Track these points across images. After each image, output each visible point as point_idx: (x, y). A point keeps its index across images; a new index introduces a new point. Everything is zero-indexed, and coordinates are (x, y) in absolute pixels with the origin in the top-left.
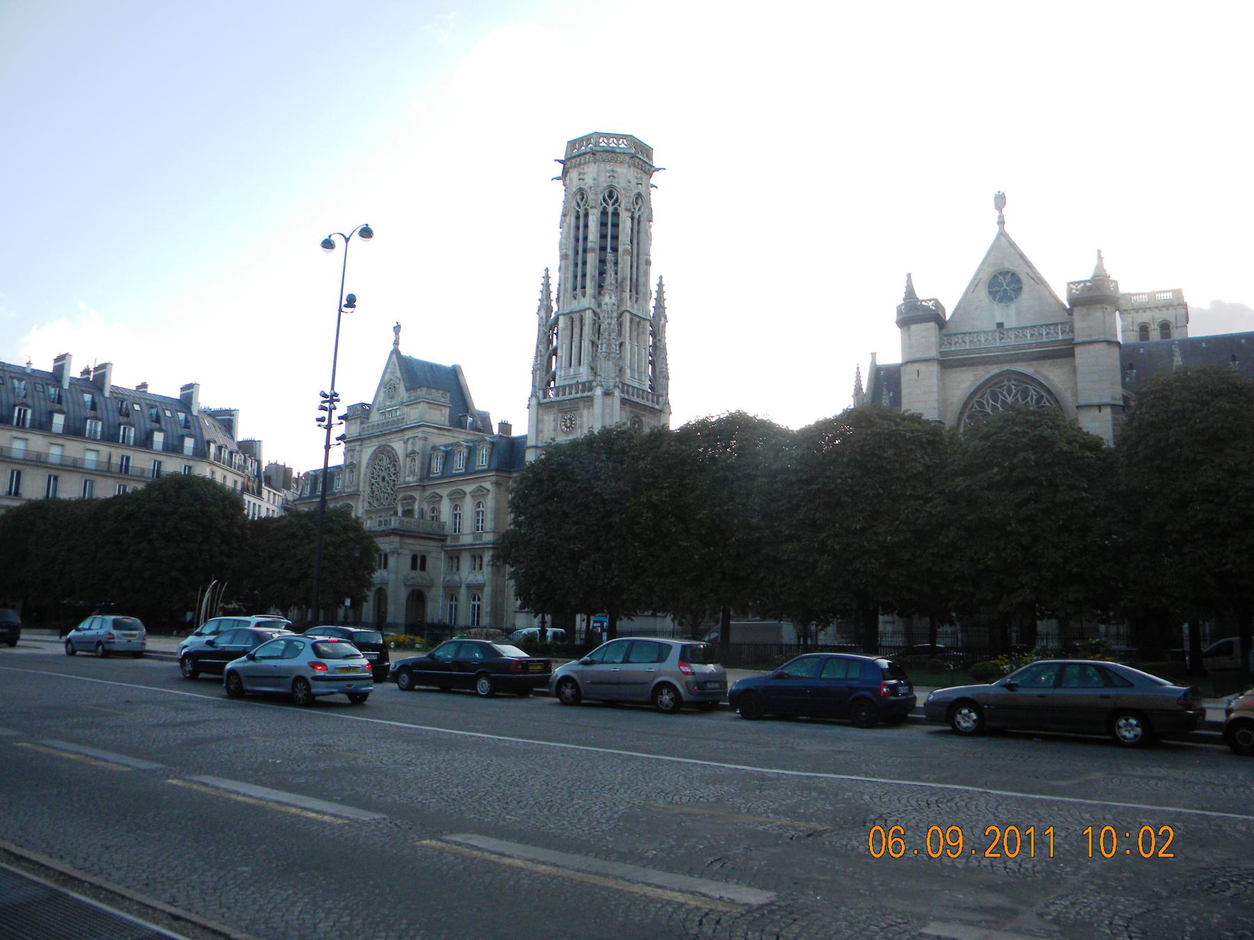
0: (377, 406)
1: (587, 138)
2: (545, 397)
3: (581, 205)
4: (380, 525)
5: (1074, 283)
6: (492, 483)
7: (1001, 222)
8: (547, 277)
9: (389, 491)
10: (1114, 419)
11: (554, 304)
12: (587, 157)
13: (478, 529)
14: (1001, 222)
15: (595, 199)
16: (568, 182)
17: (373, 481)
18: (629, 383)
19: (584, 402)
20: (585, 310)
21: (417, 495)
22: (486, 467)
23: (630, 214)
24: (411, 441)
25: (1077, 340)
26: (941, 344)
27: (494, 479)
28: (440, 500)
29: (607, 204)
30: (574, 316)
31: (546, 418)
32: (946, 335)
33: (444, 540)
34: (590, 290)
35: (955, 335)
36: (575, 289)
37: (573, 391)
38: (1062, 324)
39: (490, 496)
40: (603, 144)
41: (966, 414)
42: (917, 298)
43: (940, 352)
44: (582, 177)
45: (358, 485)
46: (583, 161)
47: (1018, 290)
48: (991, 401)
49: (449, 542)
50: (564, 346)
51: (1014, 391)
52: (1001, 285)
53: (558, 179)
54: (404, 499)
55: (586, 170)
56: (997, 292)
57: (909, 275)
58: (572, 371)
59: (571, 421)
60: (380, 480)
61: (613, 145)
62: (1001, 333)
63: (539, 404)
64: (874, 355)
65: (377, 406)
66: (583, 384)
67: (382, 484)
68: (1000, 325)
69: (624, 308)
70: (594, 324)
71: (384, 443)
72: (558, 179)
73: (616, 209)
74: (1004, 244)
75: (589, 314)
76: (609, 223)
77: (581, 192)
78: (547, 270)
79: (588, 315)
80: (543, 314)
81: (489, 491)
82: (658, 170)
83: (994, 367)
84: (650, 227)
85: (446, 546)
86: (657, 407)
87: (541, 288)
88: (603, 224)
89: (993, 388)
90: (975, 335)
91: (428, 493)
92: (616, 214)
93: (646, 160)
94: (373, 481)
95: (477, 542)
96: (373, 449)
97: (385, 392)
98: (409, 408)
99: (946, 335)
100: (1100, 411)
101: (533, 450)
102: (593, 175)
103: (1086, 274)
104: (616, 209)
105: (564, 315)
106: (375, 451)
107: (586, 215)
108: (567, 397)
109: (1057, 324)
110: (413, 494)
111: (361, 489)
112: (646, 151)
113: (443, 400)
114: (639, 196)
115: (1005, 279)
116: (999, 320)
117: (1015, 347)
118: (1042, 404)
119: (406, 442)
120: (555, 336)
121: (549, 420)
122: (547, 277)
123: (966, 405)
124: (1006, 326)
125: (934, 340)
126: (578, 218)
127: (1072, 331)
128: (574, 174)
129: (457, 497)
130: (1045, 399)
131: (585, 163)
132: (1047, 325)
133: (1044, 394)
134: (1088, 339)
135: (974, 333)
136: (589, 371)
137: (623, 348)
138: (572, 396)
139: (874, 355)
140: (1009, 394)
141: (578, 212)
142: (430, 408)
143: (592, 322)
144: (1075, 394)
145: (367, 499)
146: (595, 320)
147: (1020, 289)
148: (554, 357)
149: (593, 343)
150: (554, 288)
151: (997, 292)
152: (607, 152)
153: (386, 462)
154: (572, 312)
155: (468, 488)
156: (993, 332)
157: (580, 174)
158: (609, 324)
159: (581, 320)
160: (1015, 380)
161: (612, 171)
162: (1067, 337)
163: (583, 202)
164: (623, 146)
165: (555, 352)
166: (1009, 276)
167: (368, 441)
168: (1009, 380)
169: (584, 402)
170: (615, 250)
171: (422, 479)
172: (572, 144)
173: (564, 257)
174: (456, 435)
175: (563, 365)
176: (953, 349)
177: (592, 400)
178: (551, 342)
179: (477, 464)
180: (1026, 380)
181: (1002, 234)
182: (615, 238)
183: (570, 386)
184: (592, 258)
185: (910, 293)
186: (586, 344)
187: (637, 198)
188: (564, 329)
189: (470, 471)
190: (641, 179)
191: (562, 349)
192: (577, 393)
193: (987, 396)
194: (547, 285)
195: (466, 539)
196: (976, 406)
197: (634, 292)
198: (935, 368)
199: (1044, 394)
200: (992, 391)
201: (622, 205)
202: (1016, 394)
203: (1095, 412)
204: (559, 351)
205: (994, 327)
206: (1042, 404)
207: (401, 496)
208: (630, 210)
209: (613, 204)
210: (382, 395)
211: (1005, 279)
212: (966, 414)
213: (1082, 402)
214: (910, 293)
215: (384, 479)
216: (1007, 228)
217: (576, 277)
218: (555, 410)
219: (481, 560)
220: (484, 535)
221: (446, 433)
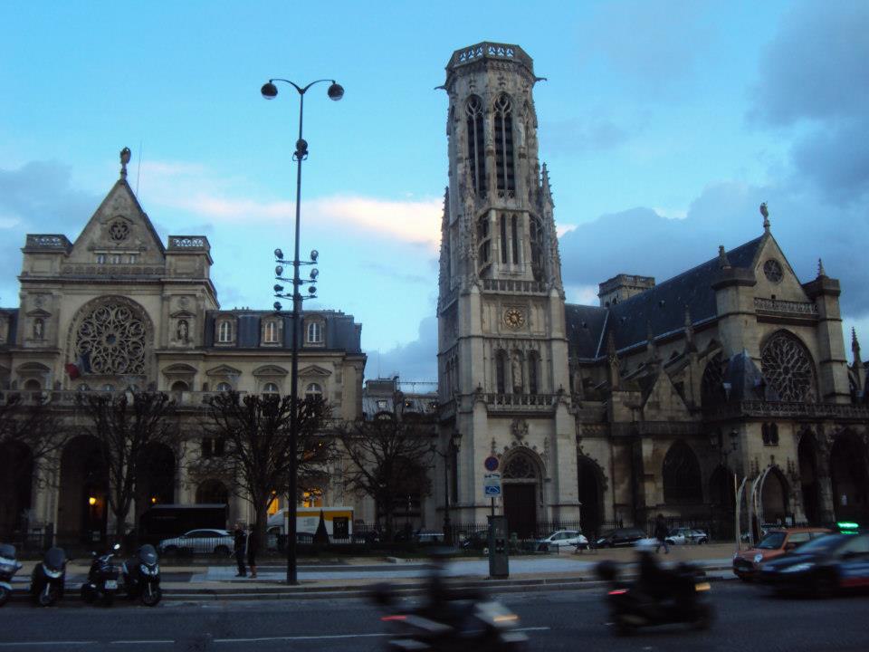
7: (766, 225)
12: (511, 65)
14: (766, 225)
17: (86, 339)
20: (522, 212)
21: (201, 366)
30: (507, 214)
31: (486, 308)
37: (523, 289)
40: (492, 53)
45: (56, 340)
75: (526, 216)
94: (86, 339)
96: (89, 298)
105: (497, 210)
106: (94, 300)
110: (192, 364)
111: (60, 346)
119: (165, 299)
124: (777, 298)
138: (518, 293)
154: (505, 210)
159: (514, 219)
167: (76, 287)
169: (533, 301)
216: (772, 230)
218: (500, 304)
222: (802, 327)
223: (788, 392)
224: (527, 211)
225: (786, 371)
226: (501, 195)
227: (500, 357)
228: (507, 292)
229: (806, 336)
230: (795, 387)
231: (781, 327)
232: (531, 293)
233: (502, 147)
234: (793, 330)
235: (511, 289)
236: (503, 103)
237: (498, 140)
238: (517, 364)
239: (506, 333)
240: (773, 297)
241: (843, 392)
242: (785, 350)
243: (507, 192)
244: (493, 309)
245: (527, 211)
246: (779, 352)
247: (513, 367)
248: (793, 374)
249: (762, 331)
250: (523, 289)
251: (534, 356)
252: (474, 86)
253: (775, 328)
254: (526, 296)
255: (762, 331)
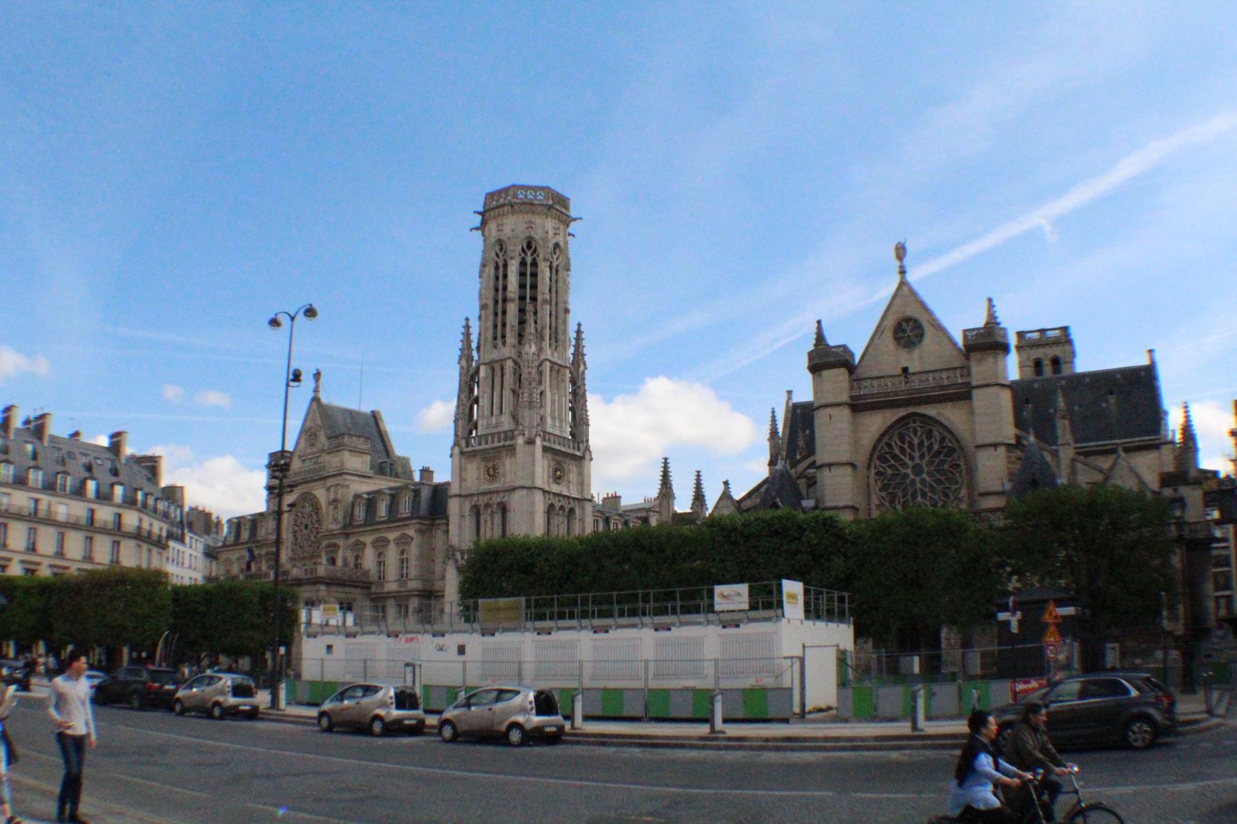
0: (298, 453)
1: (506, 190)
2: (467, 446)
3: (500, 255)
4: (306, 573)
5: (968, 330)
6: (416, 531)
7: (903, 272)
8: (467, 327)
9: (313, 539)
10: (1008, 457)
11: (475, 354)
12: (506, 209)
13: (403, 577)
14: (903, 272)
15: (515, 249)
16: (486, 232)
17: (296, 528)
18: (550, 430)
19: (507, 450)
20: (506, 359)
21: (340, 542)
22: (409, 515)
23: (548, 264)
24: (332, 489)
25: (974, 383)
26: (852, 388)
27: (417, 526)
28: (364, 547)
29: (526, 254)
31: (469, 466)
32: (855, 380)
33: (369, 588)
34: (511, 339)
35: (865, 379)
36: (495, 338)
37: (496, 440)
38: (961, 368)
39: (414, 544)
40: (521, 196)
41: (876, 455)
42: (828, 345)
43: (851, 397)
44: (500, 228)
46: (501, 213)
47: (921, 336)
48: (898, 443)
49: (373, 589)
50: (486, 395)
51: (919, 433)
52: (904, 331)
53: (477, 229)
54: (329, 546)
55: (504, 221)
56: (902, 338)
57: (819, 322)
58: (494, 420)
59: (494, 470)
60: (303, 527)
61: (531, 197)
62: (905, 377)
63: (462, 453)
64: (790, 393)
65: (298, 453)
66: (505, 432)
67: (305, 532)
68: (905, 370)
69: (543, 357)
70: (515, 373)
71: (305, 490)
72: (477, 229)
73: (534, 260)
74: (904, 291)
76: (529, 274)
77: (501, 244)
78: (467, 319)
79: (509, 364)
80: (464, 363)
81: (412, 538)
82: (575, 220)
83: (902, 409)
84: (568, 275)
85: (371, 594)
86: (578, 453)
87: (461, 337)
88: (522, 274)
89: (900, 430)
90: (883, 380)
91: (352, 540)
92: (534, 264)
93: (563, 210)
94: (296, 528)
95: (402, 590)
97: (306, 440)
98: (331, 455)
99: (855, 380)
100: (996, 450)
101: (457, 498)
102: (513, 226)
103: (979, 321)
104: (534, 260)
107: (505, 266)
108: (490, 445)
109: (956, 368)
112: (563, 201)
113: (364, 447)
114: (557, 245)
115: (908, 325)
116: (906, 365)
117: (919, 391)
118: (944, 445)
119: (328, 490)
120: (476, 385)
121: (474, 470)
122: (467, 327)
123: (875, 448)
124: (911, 371)
125: (846, 385)
126: (497, 268)
127: (969, 374)
128: (492, 226)
129: (381, 544)
130: (947, 441)
131: (503, 215)
132: (947, 369)
133: (946, 434)
134: (984, 382)
135: (882, 377)
136: (511, 419)
137: (543, 396)
139: (790, 393)
140: (916, 435)
141: (497, 263)
142: (352, 455)
143: (512, 371)
144: (973, 434)
145: (290, 545)
146: (515, 369)
147: (922, 335)
148: (475, 406)
149: (514, 392)
150: (474, 337)
151: (902, 338)
152: (524, 204)
153: (308, 509)
155: (392, 536)
156: (900, 376)
157: (498, 225)
158: (530, 373)
159: (502, 369)
160: (921, 422)
161: (530, 222)
162: (965, 380)
163: (502, 253)
164: (540, 197)
165: (476, 401)
166: (911, 324)
168: (914, 422)
170: (534, 299)
171: (344, 527)
172: (490, 196)
173: (483, 307)
174: (377, 482)
175: (485, 415)
176: (862, 393)
177: (514, 449)
178: (472, 390)
179: (400, 511)
180: (929, 422)
181: (903, 283)
182: (534, 287)
183: (493, 435)
184: (512, 308)
185: (820, 338)
186: (507, 393)
187: (555, 248)
188: (485, 378)
189: (394, 518)
190: (559, 229)
191: (483, 398)
192: (499, 441)
193: (896, 438)
194: (467, 335)
195: (391, 587)
196: (885, 448)
197: (553, 341)
198: (846, 411)
199: (946, 434)
200: (900, 433)
201: (541, 256)
202: (921, 436)
203: (991, 451)
204: (481, 400)
205: (900, 372)
206: (944, 445)
207: (325, 543)
208: (548, 260)
209: (532, 255)
210: (302, 443)
211: (908, 325)
212: (876, 455)
213: (980, 441)
214: (820, 338)
215: (306, 526)
217: (496, 326)
219: (407, 608)
220: (409, 582)
221: (368, 480)
222: (950, 404)
223: (919, 498)
224: (510, 358)
225: (918, 470)
226: (495, 347)
227: (477, 511)
228: (483, 447)
229: (951, 415)
230: (933, 490)
231: (912, 410)
232: (501, 444)
233: (526, 293)
234: (930, 411)
235: (487, 443)
236: (501, 250)
237: (522, 286)
238: (489, 518)
239: (485, 487)
240: (905, 370)
241: (994, 489)
242: (916, 441)
243: (499, 341)
244: (475, 465)
245: (510, 358)
246: (906, 446)
247: (486, 522)
248: (906, 476)
249: (875, 423)
250: (496, 440)
251: (504, 509)
252: (502, 230)
253: (902, 412)
254: (498, 447)
255: (875, 423)
